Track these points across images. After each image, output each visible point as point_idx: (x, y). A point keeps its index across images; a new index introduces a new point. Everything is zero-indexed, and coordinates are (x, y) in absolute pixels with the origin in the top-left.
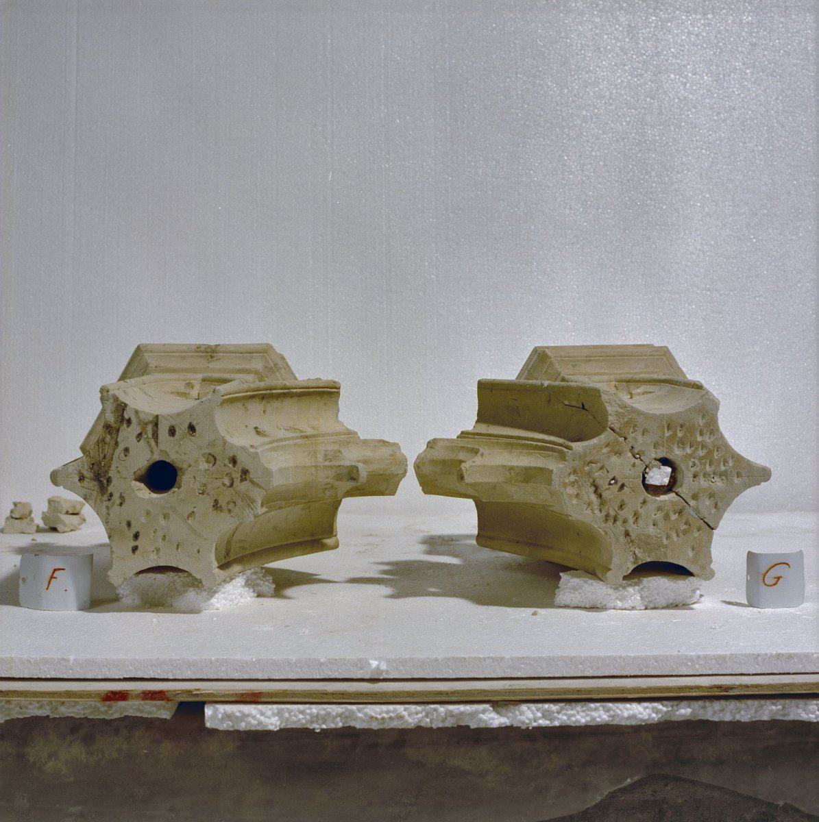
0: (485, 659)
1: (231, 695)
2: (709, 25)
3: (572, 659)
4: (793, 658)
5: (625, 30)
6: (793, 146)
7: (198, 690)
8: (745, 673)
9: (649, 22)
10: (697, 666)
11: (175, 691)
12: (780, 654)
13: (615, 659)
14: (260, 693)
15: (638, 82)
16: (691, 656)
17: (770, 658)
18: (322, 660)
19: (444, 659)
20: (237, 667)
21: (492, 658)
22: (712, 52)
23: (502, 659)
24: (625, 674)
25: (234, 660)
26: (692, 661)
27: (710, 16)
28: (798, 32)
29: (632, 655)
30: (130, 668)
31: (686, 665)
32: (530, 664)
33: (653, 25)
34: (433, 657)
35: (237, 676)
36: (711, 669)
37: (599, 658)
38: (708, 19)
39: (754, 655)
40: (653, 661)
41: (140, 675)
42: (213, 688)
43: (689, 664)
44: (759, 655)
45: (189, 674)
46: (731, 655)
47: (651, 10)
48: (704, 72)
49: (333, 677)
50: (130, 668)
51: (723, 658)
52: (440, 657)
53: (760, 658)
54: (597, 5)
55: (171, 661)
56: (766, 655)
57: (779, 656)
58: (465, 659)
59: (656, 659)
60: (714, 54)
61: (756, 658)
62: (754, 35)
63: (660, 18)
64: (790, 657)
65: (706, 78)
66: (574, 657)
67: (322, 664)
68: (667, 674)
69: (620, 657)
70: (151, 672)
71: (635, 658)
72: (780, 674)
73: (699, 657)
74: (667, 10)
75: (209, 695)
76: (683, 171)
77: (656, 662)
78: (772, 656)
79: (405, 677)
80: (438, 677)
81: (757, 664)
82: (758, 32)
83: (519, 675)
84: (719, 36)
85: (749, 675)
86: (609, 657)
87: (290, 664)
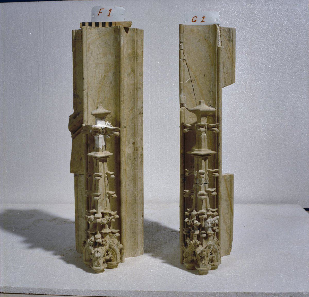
0: (146, 291)
2: (270, 26)
3: (175, 292)
4: (249, 294)
5: (239, 28)
6: (301, 71)
9: (248, 26)
12: (245, 293)
13: (189, 293)
15: (243, 48)
16: (215, 292)
22: (271, 36)
23: (152, 291)
27: (271, 23)
28: (304, 28)
29: (195, 292)
32: (161, 293)
33: (249, 27)
37: (184, 292)
38: (270, 24)
39: (236, 292)
43: (214, 295)
44: (238, 293)
46: (228, 292)
47: (248, 21)
48: (268, 44)
51: (226, 293)
53: (238, 294)
54: (229, 20)
58: (139, 291)
60: (272, 37)
61: (236, 294)
62: (287, 29)
63: (252, 24)
65: (268, 46)
69: (191, 292)
71: (196, 293)
73: (217, 293)
74: (254, 21)
76: (259, 81)
77: (203, 294)
78: (242, 293)
82: (289, 28)
84: (274, 30)
86: (187, 292)
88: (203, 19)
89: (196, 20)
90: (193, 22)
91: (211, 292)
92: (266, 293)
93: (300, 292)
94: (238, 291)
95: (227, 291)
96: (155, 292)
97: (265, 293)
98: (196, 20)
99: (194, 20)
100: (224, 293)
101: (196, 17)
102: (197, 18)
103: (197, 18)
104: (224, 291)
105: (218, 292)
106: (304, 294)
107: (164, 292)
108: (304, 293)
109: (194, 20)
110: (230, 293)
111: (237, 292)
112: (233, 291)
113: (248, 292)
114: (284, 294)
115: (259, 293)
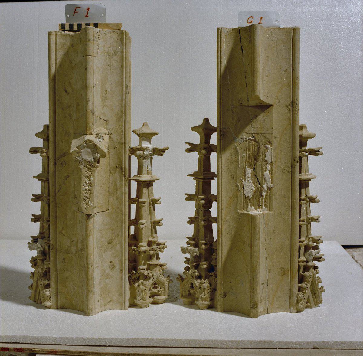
0: (146, 339)
1: (46, 351)
4: (266, 343)
7: (34, 349)
8: (247, 348)
10: (228, 345)
11: (26, 349)
12: (261, 341)
13: (196, 341)
14: (56, 351)
16: (226, 340)
17: (257, 342)
18: (85, 338)
19: (131, 339)
20: (54, 340)
21: (149, 339)
23: (153, 339)
24: (200, 347)
25: (52, 337)
26: (226, 342)
30: (14, 339)
31: (224, 344)
34: (127, 338)
35: (53, 343)
36: (234, 346)
37: (190, 340)
39: (250, 341)
40: (211, 342)
41: (18, 341)
42: (40, 348)
44: (252, 341)
45: (36, 342)
49: (89, 344)
50: (14, 339)
51: (238, 342)
52: (129, 338)
53: (253, 342)
55: (29, 336)
56: (255, 341)
57: (260, 342)
59: (212, 341)
61: (251, 342)
64: (265, 342)
66: (181, 339)
67: (85, 340)
68: (217, 347)
70: (22, 341)
71: (204, 340)
72: (266, 349)
73: (229, 341)
75: (38, 351)
77: (212, 342)
79: (116, 345)
80: (129, 345)
81: (252, 345)
83: (159, 345)
85: (248, 348)
87: (73, 339)
88: (261, 20)
89: (252, 21)
90: (248, 23)
91: (222, 339)
92: (285, 342)
93: (325, 340)
94: (253, 340)
95: (241, 340)
96: (156, 339)
97: (285, 341)
98: (252, 21)
99: (249, 21)
100: (237, 341)
101: (252, 17)
102: (253, 18)
103: (253, 18)
104: (237, 339)
105: (230, 339)
106: (329, 343)
107: (167, 339)
108: (330, 342)
109: (249, 21)
110: (243, 342)
111: (251, 340)
112: (247, 339)
113: (265, 341)
114: (306, 343)
115: (277, 341)
